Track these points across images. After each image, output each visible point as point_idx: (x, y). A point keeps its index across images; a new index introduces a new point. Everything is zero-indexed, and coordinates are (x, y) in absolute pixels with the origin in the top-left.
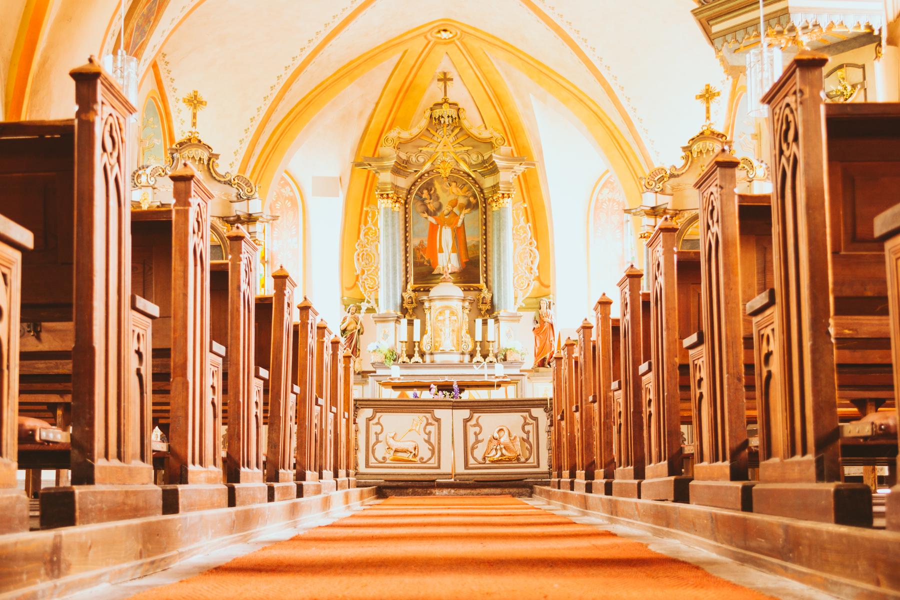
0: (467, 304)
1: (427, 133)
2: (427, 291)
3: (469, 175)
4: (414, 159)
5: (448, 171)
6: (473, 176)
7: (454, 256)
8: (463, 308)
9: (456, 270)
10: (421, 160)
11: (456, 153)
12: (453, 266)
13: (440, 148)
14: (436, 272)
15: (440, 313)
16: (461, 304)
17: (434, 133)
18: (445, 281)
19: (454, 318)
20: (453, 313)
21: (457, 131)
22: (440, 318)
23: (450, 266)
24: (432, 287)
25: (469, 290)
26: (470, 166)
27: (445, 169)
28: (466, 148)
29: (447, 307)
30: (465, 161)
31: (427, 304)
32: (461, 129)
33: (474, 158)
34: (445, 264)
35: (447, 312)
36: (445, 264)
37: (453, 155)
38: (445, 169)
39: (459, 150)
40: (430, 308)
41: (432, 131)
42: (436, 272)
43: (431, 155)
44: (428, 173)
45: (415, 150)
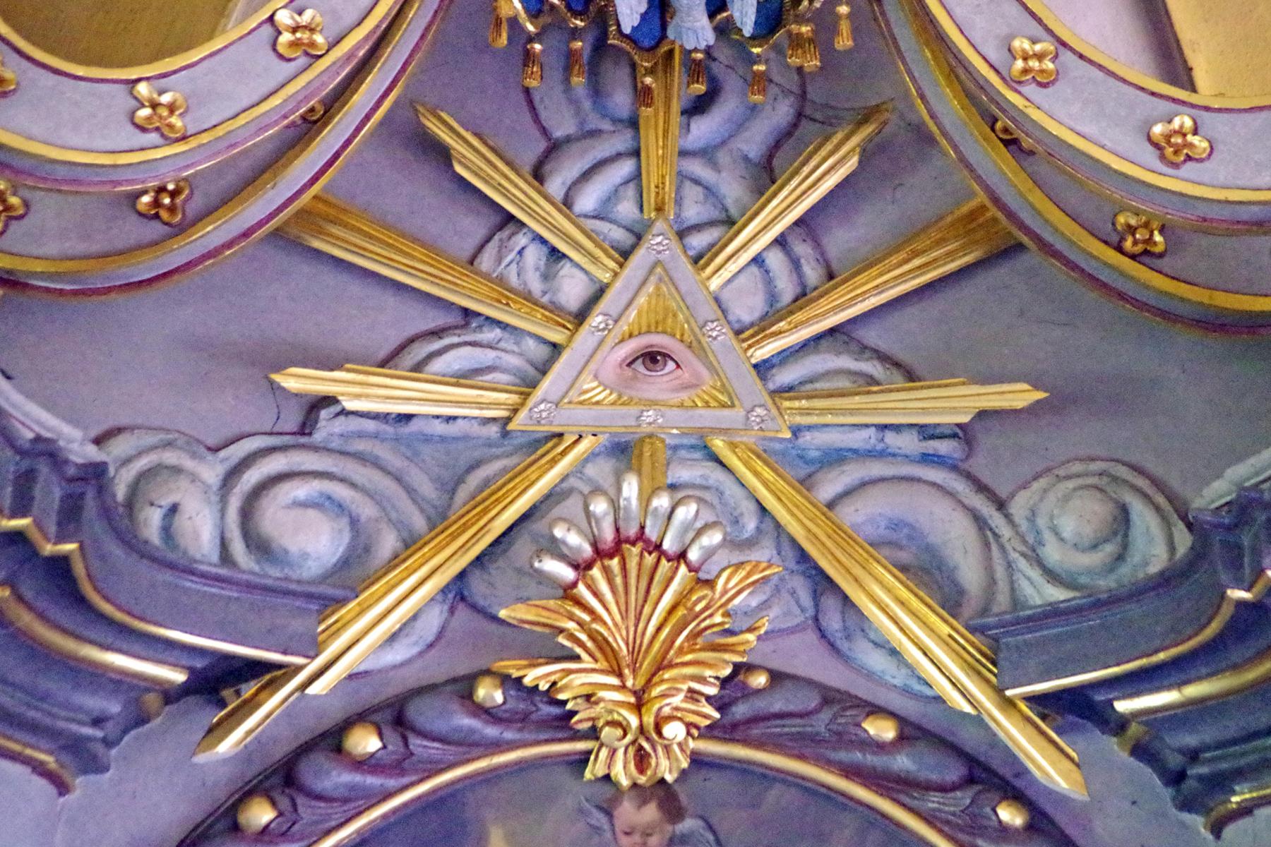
1: (408, 192)
3: (991, 775)
4: (201, 529)
5: (683, 704)
6: (1048, 763)
10: (314, 543)
11: (806, 468)
13: (586, 390)
17: (511, 192)
21: (827, 170)
26: (1001, 640)
27: (643, 673)
28: (954, 403)
30: (928, 574)
32: (898, 150)
33: (1065, 534)
37: (763, 483)
38: (643, 673)
39: (841, 420)
41: (472, 162)
43: (453, 474)
44: (395, 715)
45: (227, 407)
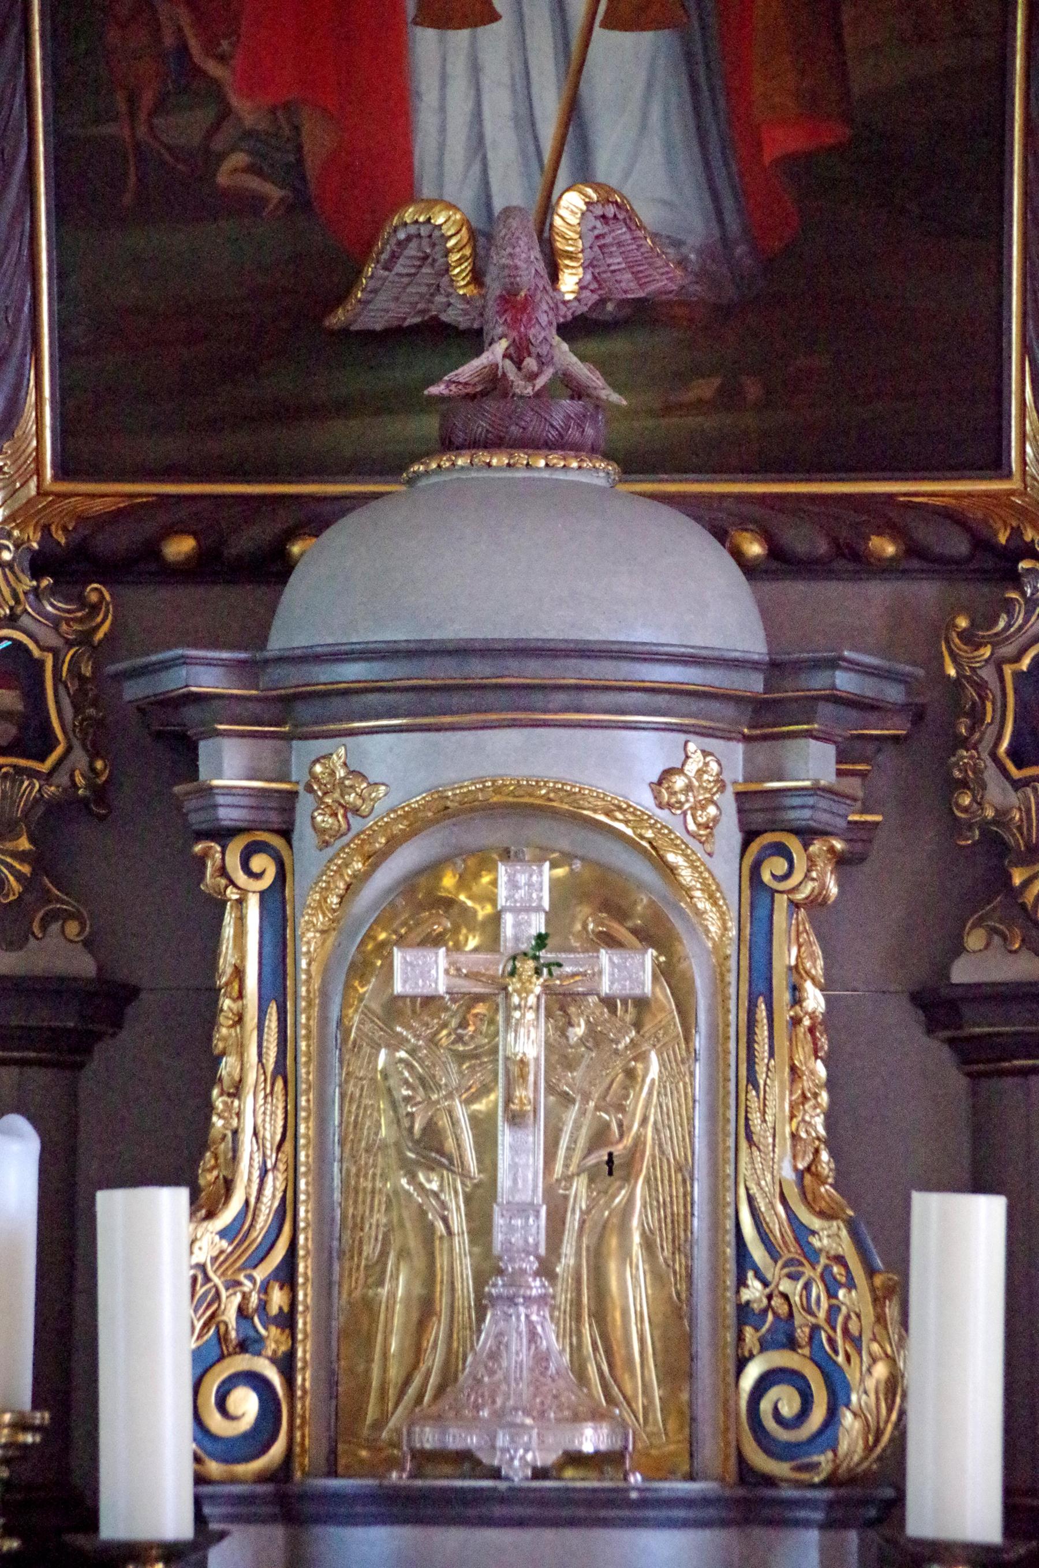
0: (813, 763)
2: (253, 565)
7: (630, 67)
8: (761, 818)
9: (664, 280)
12: (612, 212)
14: (379, 299)
15: (424, 909)
16: (713, 765)
18: (492, 422)
19: (625, 971)
20: (614, 901)
22: (423, 971)
23: (571, 205)
24: (316, 519)
25: (850, 560)
29: (524, 816)
31: (230, 769)
34: (511, 190)
35: (523, 894)
36: (511, 190)
40: (276, 819)
42: (379, 299)
